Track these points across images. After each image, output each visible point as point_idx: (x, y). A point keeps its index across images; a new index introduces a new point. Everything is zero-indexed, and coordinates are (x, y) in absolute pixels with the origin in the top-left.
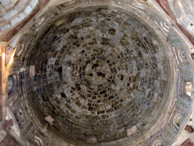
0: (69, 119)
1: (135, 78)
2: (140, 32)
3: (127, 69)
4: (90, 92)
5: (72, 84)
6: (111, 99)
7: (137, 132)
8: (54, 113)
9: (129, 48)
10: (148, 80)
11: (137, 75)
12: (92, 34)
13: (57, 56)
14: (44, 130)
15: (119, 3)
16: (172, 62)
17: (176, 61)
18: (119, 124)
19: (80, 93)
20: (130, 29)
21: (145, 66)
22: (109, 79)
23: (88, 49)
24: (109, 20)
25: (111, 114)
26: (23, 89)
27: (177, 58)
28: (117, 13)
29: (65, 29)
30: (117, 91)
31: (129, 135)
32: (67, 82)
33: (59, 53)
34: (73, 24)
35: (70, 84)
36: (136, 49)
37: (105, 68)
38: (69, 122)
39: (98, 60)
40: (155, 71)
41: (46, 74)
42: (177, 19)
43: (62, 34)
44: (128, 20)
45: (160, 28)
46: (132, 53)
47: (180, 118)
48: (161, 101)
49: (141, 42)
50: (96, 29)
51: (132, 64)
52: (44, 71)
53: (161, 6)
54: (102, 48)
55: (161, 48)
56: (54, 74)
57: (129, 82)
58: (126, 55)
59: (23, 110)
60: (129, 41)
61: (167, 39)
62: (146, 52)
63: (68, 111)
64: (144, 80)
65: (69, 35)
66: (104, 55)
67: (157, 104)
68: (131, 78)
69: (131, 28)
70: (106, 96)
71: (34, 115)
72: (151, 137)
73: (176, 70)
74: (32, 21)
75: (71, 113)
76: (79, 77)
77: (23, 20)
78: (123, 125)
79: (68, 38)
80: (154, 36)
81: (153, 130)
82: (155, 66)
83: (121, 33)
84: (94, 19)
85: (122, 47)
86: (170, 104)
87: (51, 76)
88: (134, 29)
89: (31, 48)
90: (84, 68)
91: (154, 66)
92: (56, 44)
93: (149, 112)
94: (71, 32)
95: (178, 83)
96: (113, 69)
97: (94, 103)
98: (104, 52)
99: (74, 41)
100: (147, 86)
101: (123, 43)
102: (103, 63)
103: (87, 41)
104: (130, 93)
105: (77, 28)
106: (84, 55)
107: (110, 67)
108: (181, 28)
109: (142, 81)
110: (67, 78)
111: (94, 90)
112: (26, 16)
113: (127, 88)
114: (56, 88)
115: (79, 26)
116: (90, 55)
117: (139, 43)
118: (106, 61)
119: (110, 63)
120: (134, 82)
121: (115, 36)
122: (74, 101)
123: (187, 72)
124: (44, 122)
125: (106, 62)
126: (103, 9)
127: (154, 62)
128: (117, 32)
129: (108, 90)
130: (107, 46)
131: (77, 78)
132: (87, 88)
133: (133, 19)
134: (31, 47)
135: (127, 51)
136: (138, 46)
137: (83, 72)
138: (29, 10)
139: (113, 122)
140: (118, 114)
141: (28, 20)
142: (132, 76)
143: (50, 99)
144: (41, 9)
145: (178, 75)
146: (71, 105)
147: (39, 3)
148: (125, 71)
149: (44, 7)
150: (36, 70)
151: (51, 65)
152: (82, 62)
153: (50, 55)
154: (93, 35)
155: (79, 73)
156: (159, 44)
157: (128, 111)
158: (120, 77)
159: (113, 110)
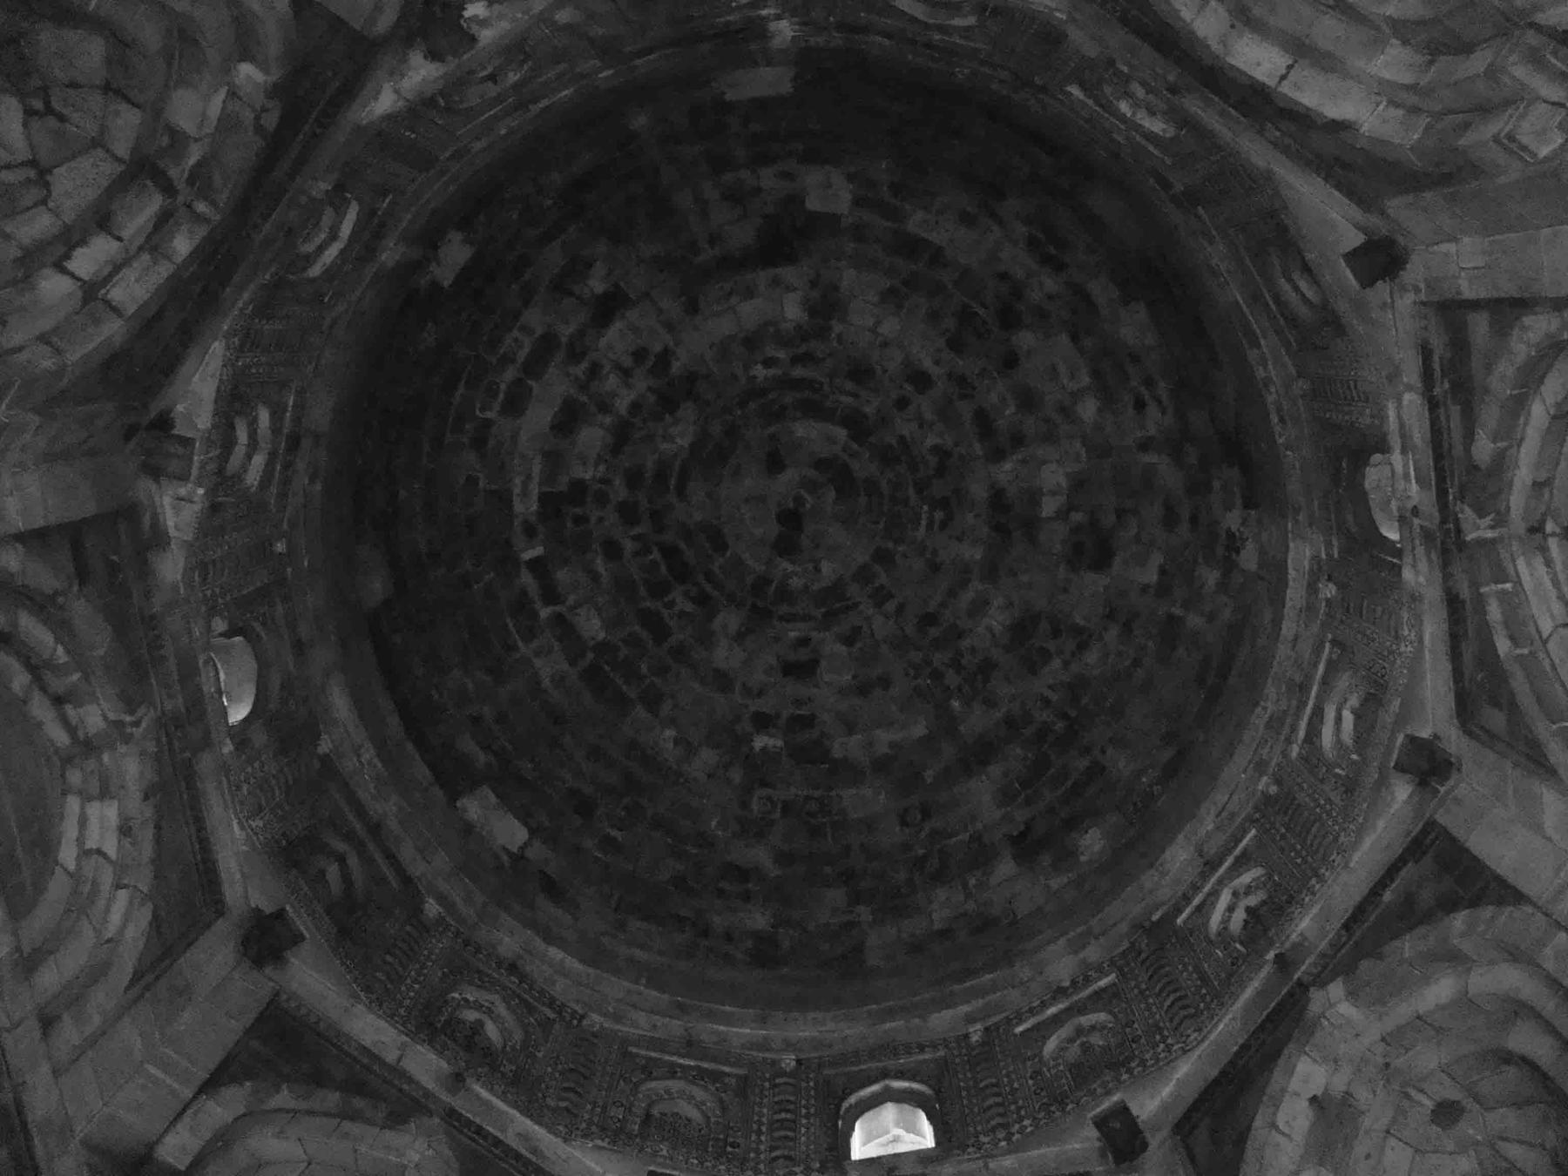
0: (461, 390)
3: (863, 690)
4: (661, 476)
5: (696, 344)
7: (497, 857)
12: (1047, 421)
14: (390, 254)
15: (1329, 590)
17: (1032, 1012)
20: (1137, 663)
24: (1170, 519)
27: (1052, 1010)
28: (1229, 566)
31: (465, 810)
34: (1101, 291)
36: (1009, 722)
37: (839, 551)
39: (884, 484)
42: (1336, 989)
43: (1021, 230)
47: (689, 1120)
53: (1392, 871)
58: (956, 664)
63: (513, 361)
65: (1019, 274)
66: (924, 523)
70: (659, 590)
72: (513, 968)
74: (1171, 78)
75: (503, 387)
84: (1156, 421)
85: (998, 628)
90: (813, 410)
95: (896, 1055)
97: (593, 520)
98: (939, 515)
103: (994, 398)
109: (813, 806)
112: (1215, 46)
116: (906, 432)
118: (890, 545)
119: (877, 568)
121: (1062, 572)
122: (583, 387)
123: (999, 1100)
124: (429, 240)
128: (1094, 583)
136: (1028, 731)
138: (1258, 59)
144: (1261, 132)
145: (946, 1043)
146: (552, 372)
148: (847, 677)
149: (1275, 145)
150: (761, 105)
152: (849, 386)
158: (803, 655)
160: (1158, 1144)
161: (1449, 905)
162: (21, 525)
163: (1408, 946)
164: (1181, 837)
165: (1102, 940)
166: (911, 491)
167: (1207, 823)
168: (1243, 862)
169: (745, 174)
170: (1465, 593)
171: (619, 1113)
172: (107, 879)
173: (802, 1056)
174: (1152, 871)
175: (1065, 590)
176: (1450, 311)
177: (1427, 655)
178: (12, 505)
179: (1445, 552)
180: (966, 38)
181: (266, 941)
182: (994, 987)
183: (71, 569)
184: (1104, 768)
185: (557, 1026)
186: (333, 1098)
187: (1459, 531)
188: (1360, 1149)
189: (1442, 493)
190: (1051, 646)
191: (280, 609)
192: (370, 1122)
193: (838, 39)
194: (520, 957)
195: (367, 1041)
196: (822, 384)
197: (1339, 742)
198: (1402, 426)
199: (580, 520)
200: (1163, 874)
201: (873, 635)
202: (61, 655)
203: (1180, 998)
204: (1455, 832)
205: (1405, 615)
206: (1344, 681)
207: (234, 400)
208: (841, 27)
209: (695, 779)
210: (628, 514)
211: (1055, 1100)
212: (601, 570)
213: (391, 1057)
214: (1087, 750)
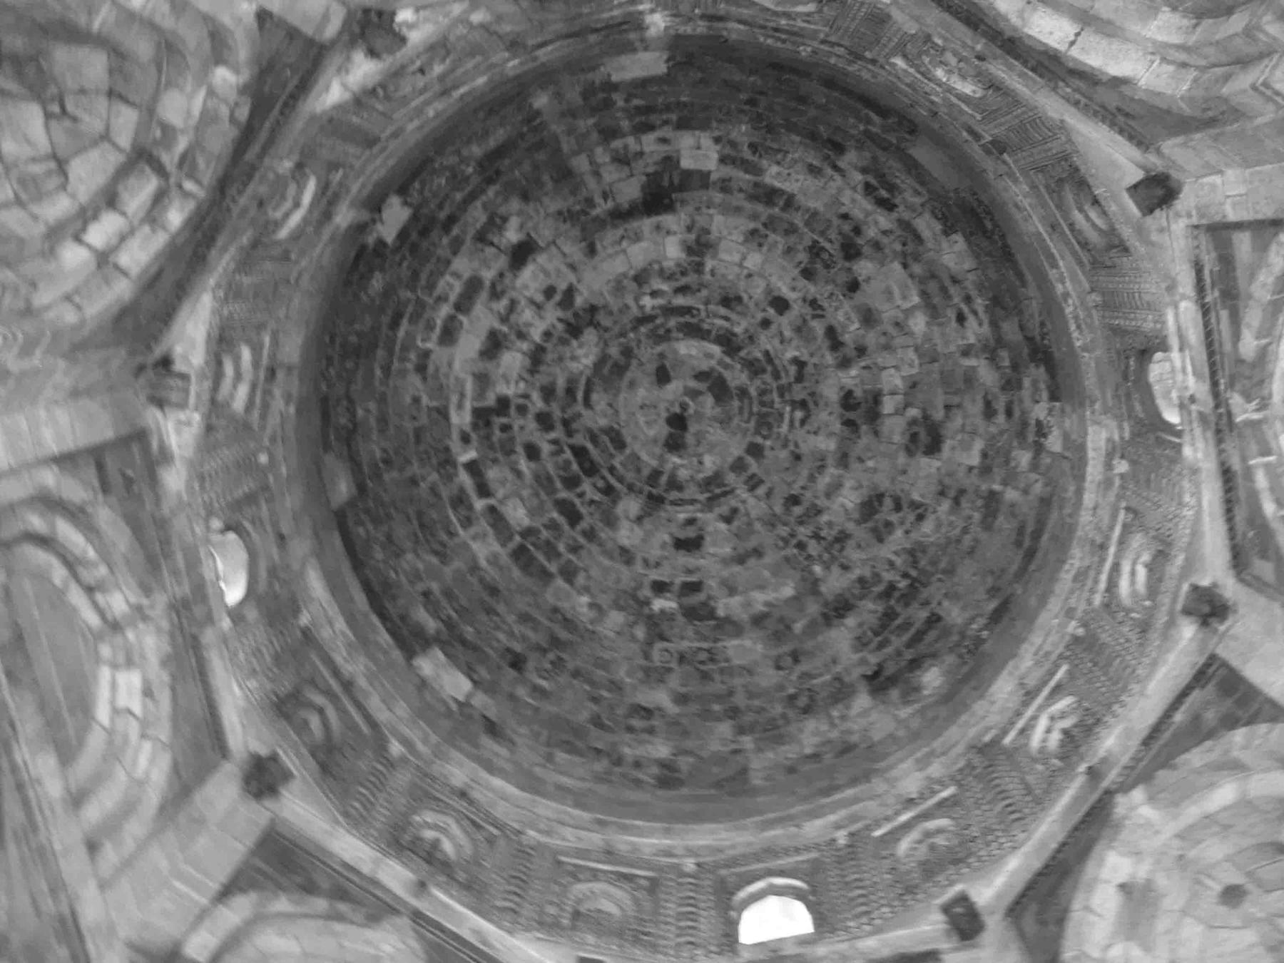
0: (404, 326)
2: (961, 589)
3: (741, 560)
4: (570, 391)
5: (594, 283)
6: (561, 513)
7: (445, 703)
8: (424, 232)
9: (859, 546)
10: (717, 687)
11: (728, 620)
12: (885, 334)
13: (728, 171)
14: (344, 217)
15: (1122, 467)
16: (871, 798)
17: (887, 819)
18: (448, 594)
19: (554, 340)
20: (965, 531)
21: (786, 648)
22: (664, 479)
23: (801, 329)
24: (989, 412)
25: (485, 535)
26: (550, 48)
27: (904, 818)
28: (1039, 448)
29: (892, 188)
30: (611, 533)
31: (420, 668)
32: (597, 258)
33: (749, 181)
34: (927, 226)
35: (588, 276)
36: (861, 580)
37: (717, 446)
38: (395, 324)
40: (778, 709)
41: (624, 136)
42: (1138, 794)
43: (858, 177)
44: (1013, 515)
45: (1039, 700)
46: (835, 570)
47: (609, 914)
48: (638, 783)
49: (907, 605)
50: (917, 349)
51: (773, 581)
52: (642, 123)
54: (821, 403)
55: (913, 715)
56: (632, 175)
58: (817, 536)
59: (442, 78)
61: (986, 745)
62: (858, 638)
64: (711, 666)
65: (857, 214)
67: (617, 770)
70: (572, 482)
71: (412, 141)
72: (463, 794)
73: (838, 826)
74: (979, 47)
76: (635, 311)
77: (995, 9)
78: (449, 617)
79: (843, 210)
80: (965, 669)
81: (493, 790)
82: (807, 704)
84: (975, 331)
86: (656, 841)
87: (612, 168)
88: (971, 552)
89: (779, 44)
90: (695, 331)
91: (803, 701)
92: (796, 155)
93: (566, 737)
94: (876, 223)
96: (719, 486)
97: (516, 428)
98: (799, 414)
99: (833, 248)
100: (683, 690)
101: (876, 504)
102: (744, 425)
103: (840, 316)
104: (620, 608)
105: (910, 248)
106: (760, 316)
107: (726, 466)
108: (1094, 823)
109: (703, 656)
111: (584, 412)
112: (1014, 20)
114: (554, 205)
115: (917, 258)
116: (769, 347)
117: (897, 594)
118: (759, 440)
119: (750, 460)
120: (684, 615)
121: (902, 459)
122: (504, 319)
124: (375, 204)
125: (749, 439)
126: (1052, 369)
127: (824, 694)
128: (928, 466)
129: (601, 484)
130: (837, 427)
131: (631, 302)
132: (588, 372)
133: (1027, 542)
134: (784, 41)
137: (669, 331)
138: (1050, 29)
139: (443, 557)
140: (492, 573)
141: (983, 27)
142: (710, 598)
143: (491, 192)
144: (1055, 89)
145: (817, 847)
147: (1104, 79)
149: (1068, 101)
150: (644, 83)
151: (678, 151)
152: (723, 311)
153: (734, 135)
154: (883, 340)
155: (661, 307)
156: (937, 703)
157: (525, 618)
158: (690, 533)
159: (511, 538)
160: (994, 925)
161: (1230, 722)
162: (54, 448)
163: (1196, 758)
164: (1005, 673)
165: (943, 759)
166: (775, 396)
167: (1026, 662)
168: (1058, 691)
169: (630, 140)
170: (1236, 464)
171: (552, 910)
172: (134, 729)
173: (701, 860)
174: (980, 702)
175: (904, 472)
176: (1219, 232)
177: (1206, 519)
178: (48, 435)
179: (1218, 431)
180: (808, 22)
181: (263, 778)
182: (856, 800)
183: (96, 483)
184: (939, 619)
185: (502, 842)
186: (321, 904)
187: (1230, 415)
188: (1162, 924)
189: (1215, 384)
190: (894, 518)
191: (264, 507)
192: (352, 923)
193: (701, 28)
194: (466, 784)
195: (347, 857)
196: (698, 310)
197: (1134, 594)
198: (1179, 329)
199: (506, 428)
200: (993, 703)
201: (748, 514)
202: (91, 553)
203: (1010, 805)
204: (1235, 662)
205: (1186, 484)
206: (1137, 540)
207: (222, 342)
208: (703, 17)
209: (606, 637)
210: (544, 421)
211: (908, 890)
213: (366, 869)
214: (926, 603)
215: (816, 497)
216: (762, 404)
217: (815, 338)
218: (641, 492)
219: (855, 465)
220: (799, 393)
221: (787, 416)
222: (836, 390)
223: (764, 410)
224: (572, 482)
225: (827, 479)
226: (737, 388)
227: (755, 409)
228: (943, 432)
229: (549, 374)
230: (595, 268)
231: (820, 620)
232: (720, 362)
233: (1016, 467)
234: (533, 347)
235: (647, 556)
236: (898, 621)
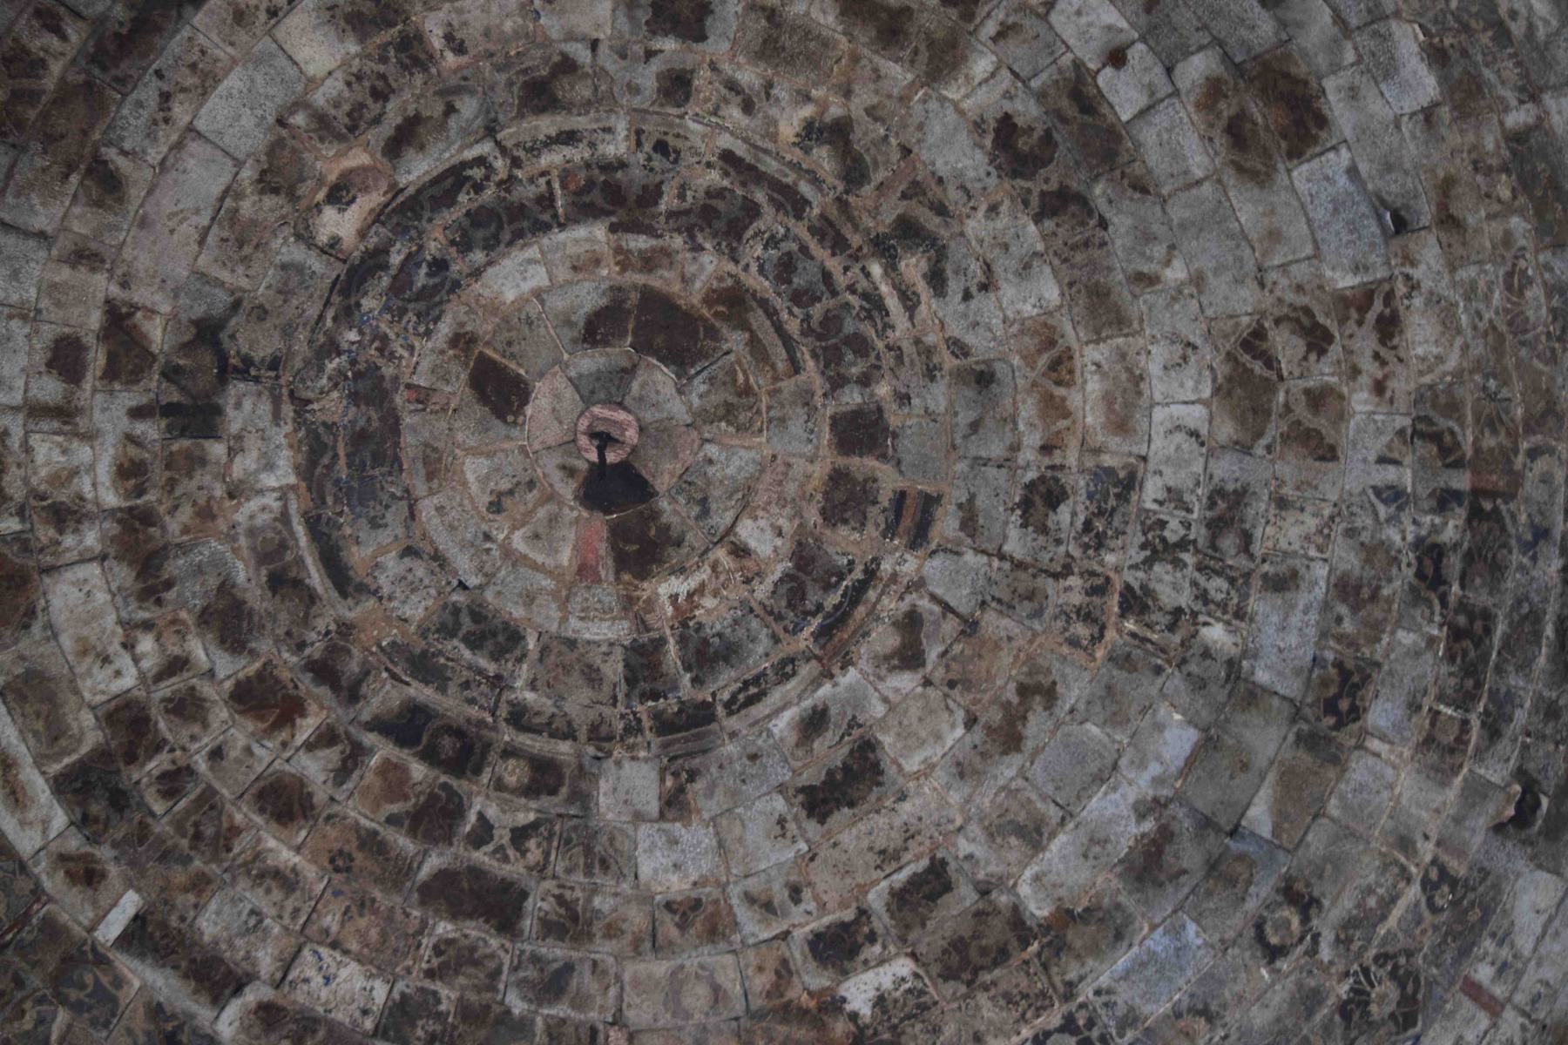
1: (996, 932)
3: (1009, 738)
4: (283, 582)
5: (168, 260)
6: (455, 915)
9: (1282, 503)
11: (1065, 917)
19: (158, 474)
20: (1515, 283)
21: (1263, 889)
32: (136, 193)
36: (1346, 589)
37: (753, 479)
46: (1259, 604)
49: (1497, 570)
51: (1122, 737)
54: (953, 195)
57: (882, 920)
58: (1160, 551)
60: (1368, 422)
62: (1429, 742)
66: (892, 303)
68: (948, 887)
69: (1535, 293)
70: (434, 819)
83: (1353, 227)
91: (1384, 996)
96: (828, 587)
97: (202, 766)
98: (913, 266)
101: (1258, 367)
102: (787, 385)
106: (648, 77)
107: (813, 516)
110: (178, 146)
113: (784, 971)
116: (725, 141)
117: (1454, 564)
118: (852, 397)
120: (948, 975)
121: (1247, 209)
129: (514, 772)
135: (1217, 526)
136: (1398, 584)
137: (439, 265)
152: (547, 125)
155: (377, 217)
158: (830, 751)
166: (820, 252)
175: (1274, 236)
190: (1325, 372)
196: (481, 161)
199: (173, 782)
201: (947, 608)
210: (265, 701)
212: (286, 857)
214: (1541, 534)
215: (1097, 451)
216: (800, 298)
217: (826, 44)
218: (633, 728)
219: (1138, 305)
220: (879, 210)
221: (884, 289)
222: (963, 139)
223: (817, 311)
224: (434, 819)
225: (1094, 386)
226: (713, 297)
227: (793, 327)
228: (1301, 70)
229: (199, 570)
230: (144, 223)
231: (1305, 758)
232: (625, 260)
233: (1531, 27)
234: (112, 528)
235: (753, 884)
236: (1501, 628)
